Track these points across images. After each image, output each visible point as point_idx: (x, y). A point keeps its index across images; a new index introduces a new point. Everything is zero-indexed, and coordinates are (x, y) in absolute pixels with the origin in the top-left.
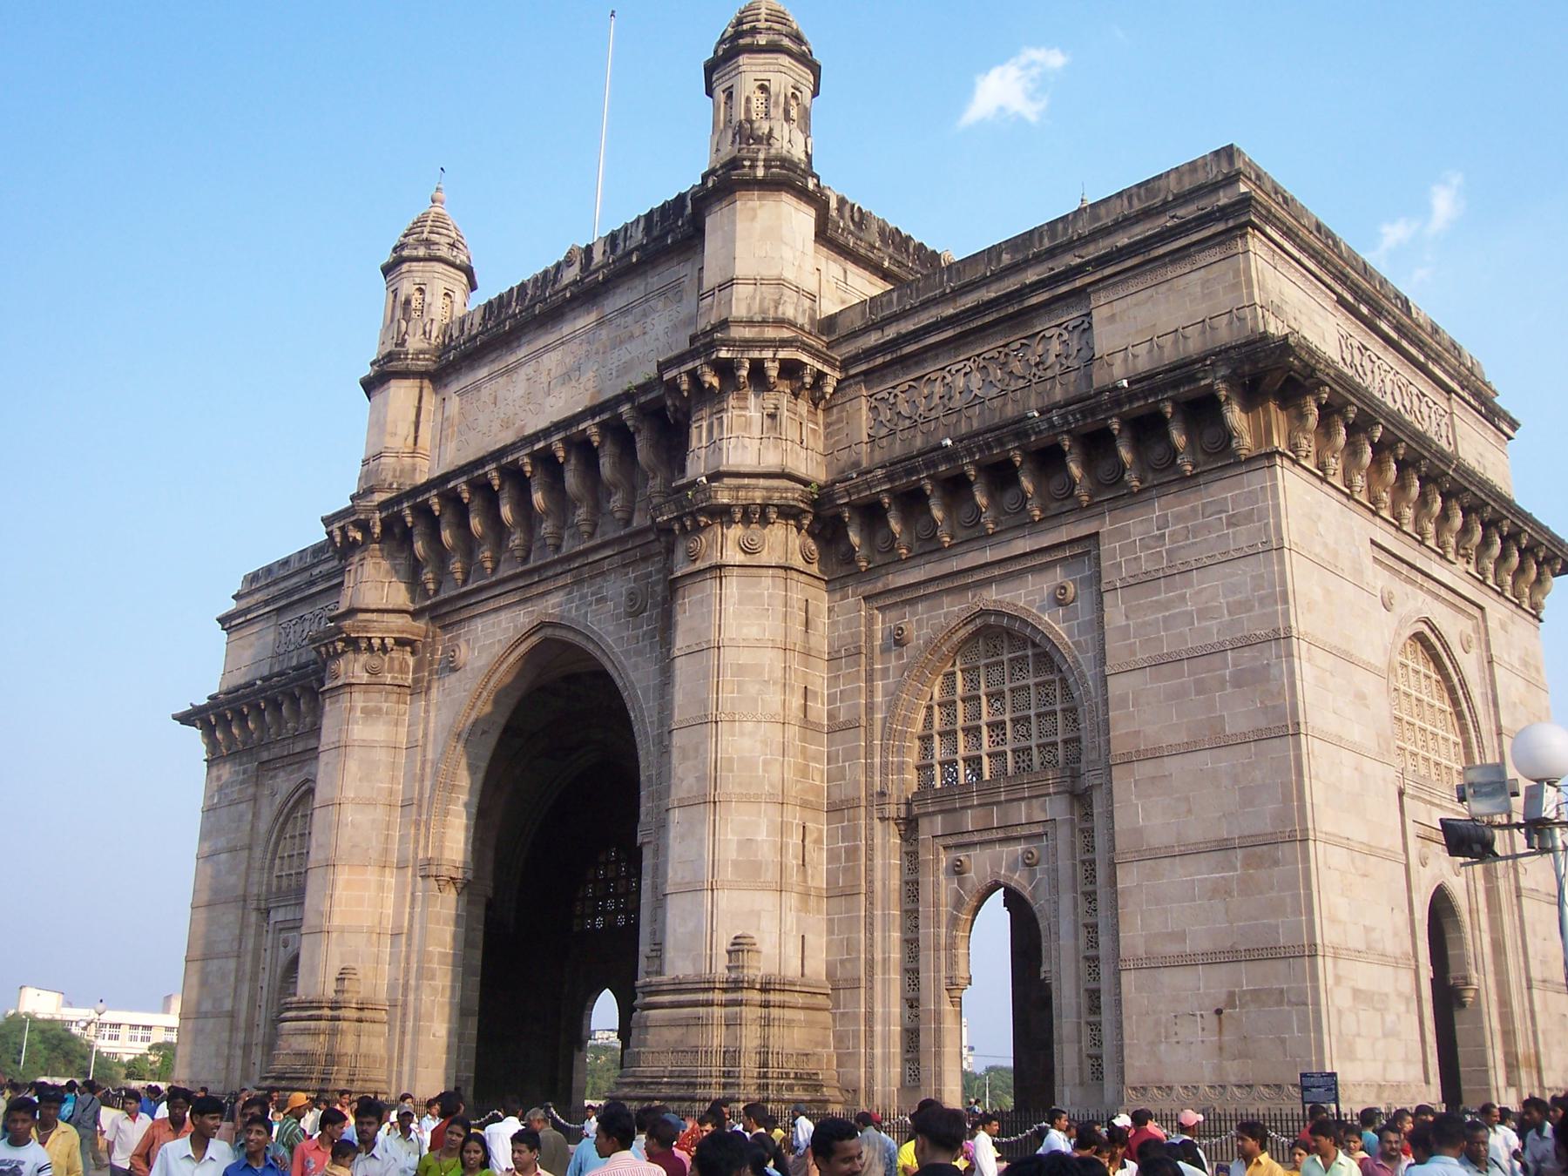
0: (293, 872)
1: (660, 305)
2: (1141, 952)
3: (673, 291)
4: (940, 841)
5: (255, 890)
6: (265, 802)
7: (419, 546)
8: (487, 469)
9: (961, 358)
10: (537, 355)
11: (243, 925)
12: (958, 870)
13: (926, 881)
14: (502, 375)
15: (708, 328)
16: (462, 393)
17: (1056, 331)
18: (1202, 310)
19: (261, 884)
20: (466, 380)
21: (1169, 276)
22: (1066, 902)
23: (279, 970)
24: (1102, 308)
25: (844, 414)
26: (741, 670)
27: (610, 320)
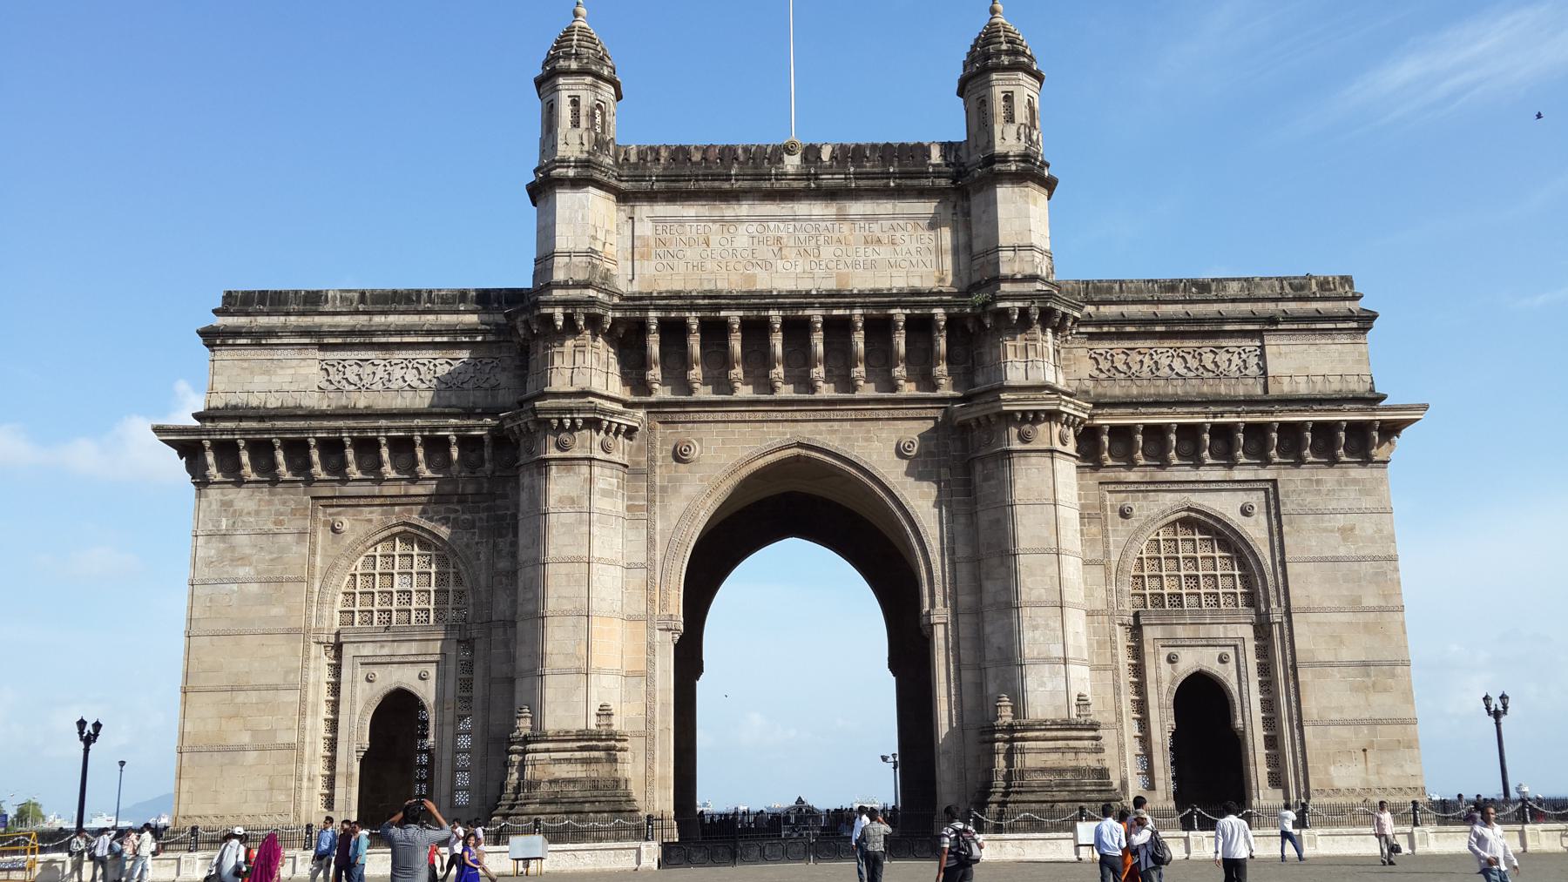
0: (374, 609)
1: (909, 227)
2: (1316, 717)
8: (771, 313)
9: (1165, 345)
10: (762, 220)
12: (1171, 660)
14: (714, 222)
15: (1019, 276)
16: (655, 220)
17: (1237, 350)
20: (662, 209)
21: (1318, 342)
24: (1273, 344)
25: (1072, 356)
27: (852, 220)
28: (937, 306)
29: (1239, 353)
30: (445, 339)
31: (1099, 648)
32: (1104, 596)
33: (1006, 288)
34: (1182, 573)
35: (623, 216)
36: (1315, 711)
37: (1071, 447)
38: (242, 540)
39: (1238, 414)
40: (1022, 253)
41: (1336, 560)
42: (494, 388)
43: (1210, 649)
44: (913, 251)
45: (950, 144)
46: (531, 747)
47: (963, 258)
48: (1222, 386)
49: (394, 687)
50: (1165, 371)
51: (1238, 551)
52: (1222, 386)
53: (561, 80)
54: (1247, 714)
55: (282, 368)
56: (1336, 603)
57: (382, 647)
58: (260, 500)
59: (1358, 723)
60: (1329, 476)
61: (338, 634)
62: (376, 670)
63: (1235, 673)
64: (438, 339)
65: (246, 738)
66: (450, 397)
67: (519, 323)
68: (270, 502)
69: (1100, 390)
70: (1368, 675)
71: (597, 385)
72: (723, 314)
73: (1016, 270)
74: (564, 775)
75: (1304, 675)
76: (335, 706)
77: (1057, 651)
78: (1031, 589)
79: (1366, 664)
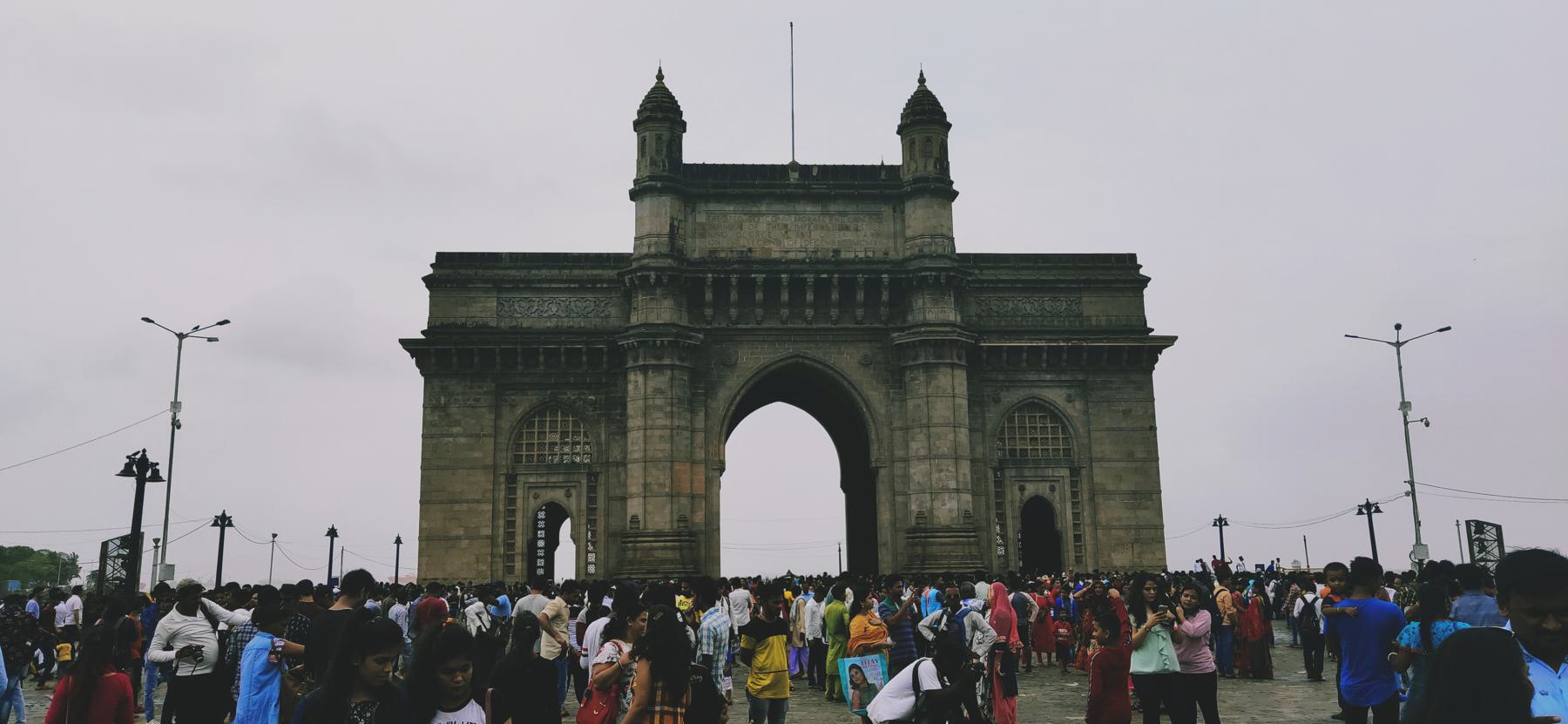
1: (866, 219)
2: (1105, 524)
3: (878, 214)
4: (1014, 479)
5: (504, 463)
6: (505, 410)
7: (709, 296)
8: (782, 276)
10: (775, 214)
11: (495, 483)
12: (1022, 489)
14: (745, 214)
16: (708, 213)
20: (713, 207)
22: (1069, 506)
23: (530, 511)
26: (960, 406)
28: (886, 272)
29: (1067, 302)
30: (577, 286)
33: (927, 263)
34: (1028, 436)
35: (688, 210)
36: (1104, 520)
37: (963, 363)
38: (454, 409)
39: (1064, 341)
40: (937, 240)
41: (1121, 429)
42: (607, 317)
44: (868, 234)
45: (892, 167)
46: (639, 539)
47: (900, 241)
48: (1056, 322)
51: (1062, 422)
52: (1056, 322)
53: (649, 125)
54: (1064, 521)
55: (475, 302)
57: (542, 477)
59: (1127, 528)
61: (514, 469)
62: (537, 491)
63: (1058, 498)
64: (572, 286)
65: (461, 532)
66: (580, 321)
67: (627, 279)
68: (471, 388)
71: (675, 320)
72: (753, 276)
73: (933, 248)
74: (660, 556)
75: (1099, 499)
76: (512, 513)
77: (953, 485)
79: (1134, 493)
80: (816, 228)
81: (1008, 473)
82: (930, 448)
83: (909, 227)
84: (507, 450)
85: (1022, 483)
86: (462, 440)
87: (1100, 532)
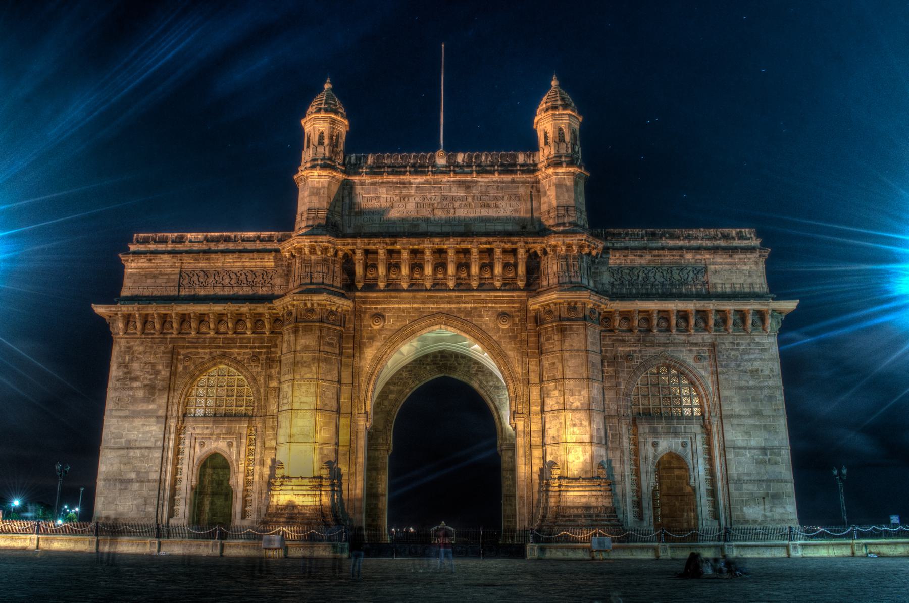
2: (736, 478)
5: (175, 414)
12: (655, 444)
13: (642, 448)
18: (749, 280)
19: (178, 411)
29: (693, 271)
31: (612, 438)
32: (616, 408)
38: (136, 366)
41: (749, 388)
42: (272, 286)
43: (676, 440)
49: (213, 451)
50: (653, 279)
54: (697, 476)
56: (748, 413)
57: (207, 428)
58: (147, 346)
60: (744, 342)
63: (691, 453)
65: (133, 476)
69: (614, 290)
70: (766, 455)
75: (731, 455)
78: (572, 403)
80: (460, 207)
81: (641, 430)
82: (564, 404)
83: (545, 203)
84: (179, 403)
85: (655, 440)
86: (140, 394)
87: (732, 486)
